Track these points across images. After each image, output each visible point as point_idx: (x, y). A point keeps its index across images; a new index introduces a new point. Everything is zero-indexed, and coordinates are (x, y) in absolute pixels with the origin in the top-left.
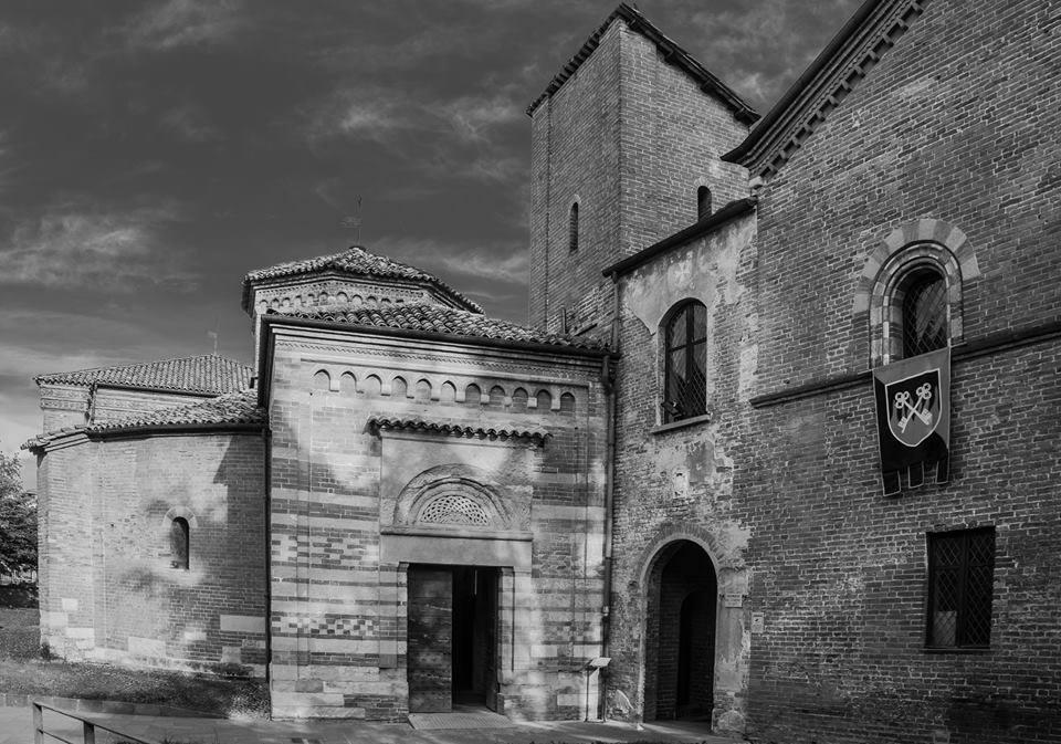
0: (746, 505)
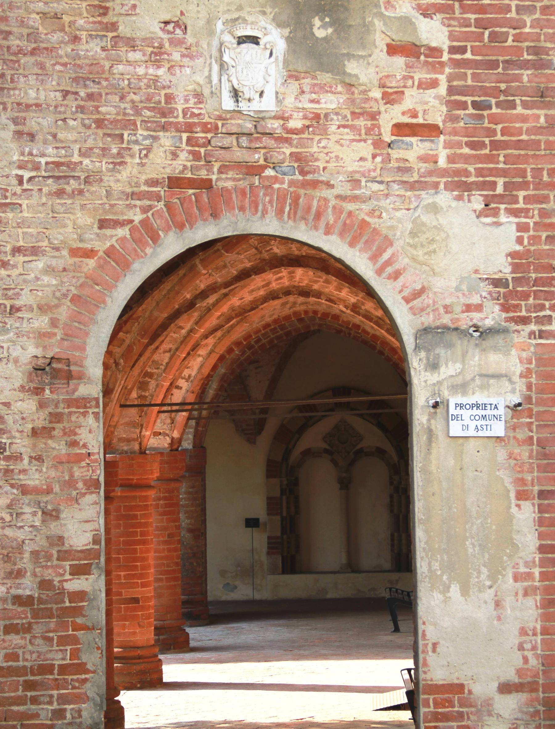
0: (491, 158)
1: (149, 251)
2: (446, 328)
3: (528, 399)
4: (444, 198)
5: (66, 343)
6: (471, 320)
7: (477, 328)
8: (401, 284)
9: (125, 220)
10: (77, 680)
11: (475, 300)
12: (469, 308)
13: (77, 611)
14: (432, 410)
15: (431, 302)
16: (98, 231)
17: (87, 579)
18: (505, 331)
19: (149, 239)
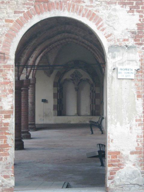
1: (29, 21)
2: (118, 46)
3: (141, 68)
4: (118, 7)
5: (4, 48)
6: (125, 43)
7: (127, 46)
8: (104, 32)
9: (22, 11)
10: (6, 149)
11: (127, 38)
12: (124, 40)
13: (7, 129)
14: (113, 70)
15: (113, 38)
16: (14, 14)
17: (9, 119)
18: (135, 47)
19: (29, 17)
